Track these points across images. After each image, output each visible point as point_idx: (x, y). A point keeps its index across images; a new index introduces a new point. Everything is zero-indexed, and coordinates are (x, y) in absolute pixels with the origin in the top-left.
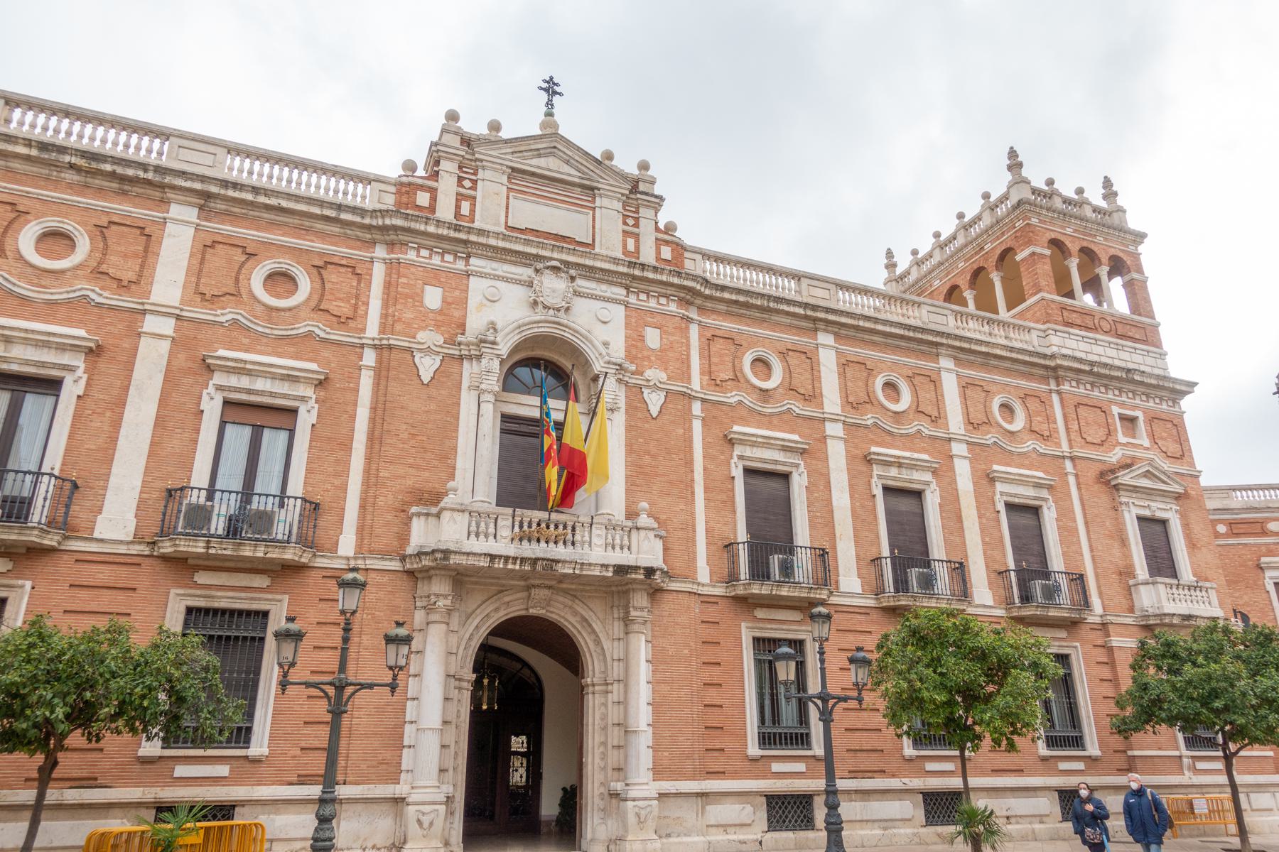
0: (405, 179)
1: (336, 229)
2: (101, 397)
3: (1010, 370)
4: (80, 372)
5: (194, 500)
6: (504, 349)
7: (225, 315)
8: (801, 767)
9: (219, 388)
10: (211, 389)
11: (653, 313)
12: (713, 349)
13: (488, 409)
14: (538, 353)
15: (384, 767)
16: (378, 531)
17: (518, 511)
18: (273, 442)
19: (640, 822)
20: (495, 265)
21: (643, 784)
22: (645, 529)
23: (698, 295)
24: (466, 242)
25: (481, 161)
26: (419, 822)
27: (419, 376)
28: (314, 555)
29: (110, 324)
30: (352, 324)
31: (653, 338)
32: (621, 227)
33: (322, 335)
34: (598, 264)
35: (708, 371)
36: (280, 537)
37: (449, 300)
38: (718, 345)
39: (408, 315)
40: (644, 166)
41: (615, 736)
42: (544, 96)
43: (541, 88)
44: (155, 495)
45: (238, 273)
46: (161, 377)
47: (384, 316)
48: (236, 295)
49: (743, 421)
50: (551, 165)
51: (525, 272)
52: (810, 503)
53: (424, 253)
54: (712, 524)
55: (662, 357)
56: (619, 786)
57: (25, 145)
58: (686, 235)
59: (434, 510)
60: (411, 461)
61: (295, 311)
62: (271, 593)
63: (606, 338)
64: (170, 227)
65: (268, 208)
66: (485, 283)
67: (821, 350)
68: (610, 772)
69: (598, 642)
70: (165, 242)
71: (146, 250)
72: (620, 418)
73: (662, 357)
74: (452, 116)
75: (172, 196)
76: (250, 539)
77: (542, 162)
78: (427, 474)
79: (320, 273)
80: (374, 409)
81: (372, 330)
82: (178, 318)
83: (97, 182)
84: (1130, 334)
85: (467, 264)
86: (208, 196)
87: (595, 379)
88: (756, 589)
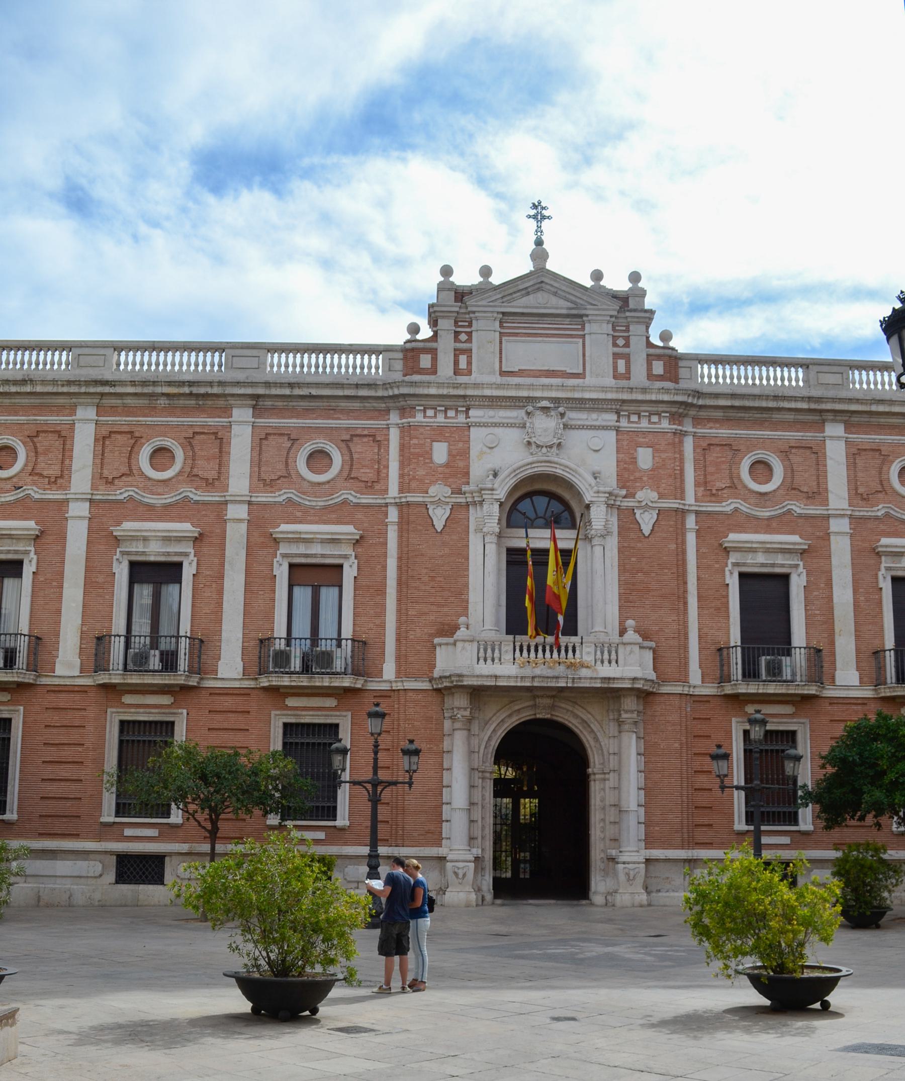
0: (409, 345)
1: (357, 405)
2: (208, 573)
4: (192, 557)
5: (277, 647)
6: (501, 493)
7: (280, 497)
8: (786, 840)
9: (284, 556)
10: (279, 558)
11: (644, 433)
12: (709, 458)
13: (491, 548)
14: (538, 486)
15: (430, 835)
16: (411, 659)
17: (518, 637)
18: (328, 595)
19: (629, 880)
20: (491, 413)
21: (633, 853)
22: (631, 644)
23: (693, 407)
24: (464, 397)
25: (474, 312)
26: (456, 874)
27: (433, 525)
28: (366, 681)
29: (206, 515)
30: (377, 487)
31: (645, 458)
32: (611, 350)
33: (355, 500)
34: (587, 395)
35: (703, 483)
36: (338, 670)
37: (454, 452)
38: (714, 455)
39: (421, 472)
40: (635, 277)
41: (612, 815)
42: (533, 223)
43: (529, 217)
44: (253, 643)
45: (287, 458)
46: (243, 553)
47: (402, 476)
48: (288, 476)
49: (741, 529)
51: (517, 415)
52: (808, 602)
53: (430, 413)
54: (705, 630)
55: (654, 477)
56: (614, 852)
57: (132, 386)
58: (681, 344)
59: (451, 640)
60: (432, 600)
61: (332, 483)
62: (339, 710)
63: (597, 468)
64: (235, 429)
65: (302, 397)
66: (484, 431)
67: (828, 442)
68: (608, 842)
69: (596, 739)
70: (234, 441)
71: (221, 452)
72: (613, 542)
73: (654, 477)
74: (447, 271)
75: (233, 402)
76: (318, 673)
77: (530, 300)
78: (446, 609)
79: (348, 447)
80: (400, 559)
81: (393, 490)
82: (250, 503)
83: (181, 402)
85: (467, 417)
86: (257, 397)
87: (588, 507)
88: (743, 689)
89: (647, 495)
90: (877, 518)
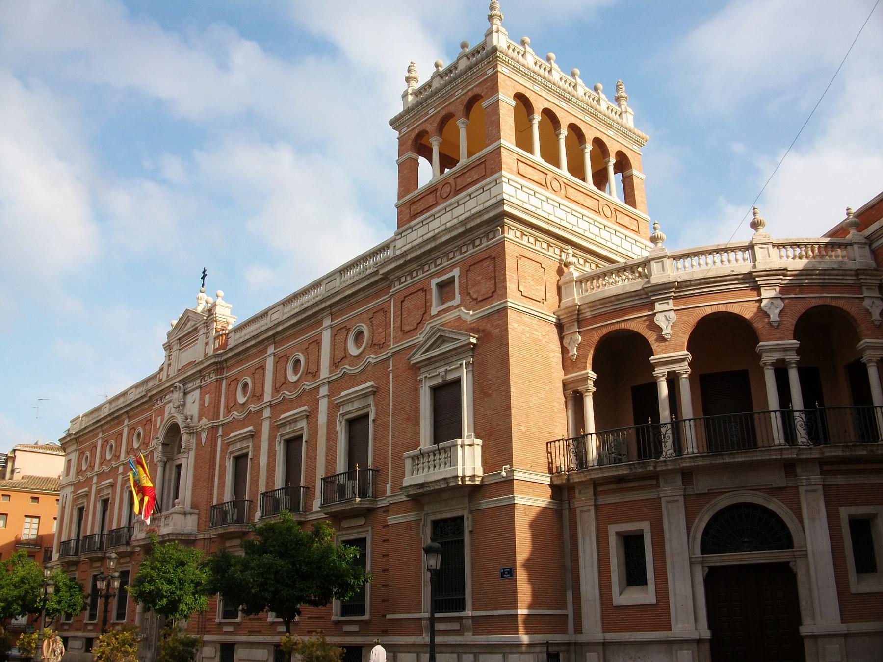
3: (366, 297)
35: (226, 407)
50: (189, 327)
84: (469, 180)
89: (204, 421)
90: (280, 402)
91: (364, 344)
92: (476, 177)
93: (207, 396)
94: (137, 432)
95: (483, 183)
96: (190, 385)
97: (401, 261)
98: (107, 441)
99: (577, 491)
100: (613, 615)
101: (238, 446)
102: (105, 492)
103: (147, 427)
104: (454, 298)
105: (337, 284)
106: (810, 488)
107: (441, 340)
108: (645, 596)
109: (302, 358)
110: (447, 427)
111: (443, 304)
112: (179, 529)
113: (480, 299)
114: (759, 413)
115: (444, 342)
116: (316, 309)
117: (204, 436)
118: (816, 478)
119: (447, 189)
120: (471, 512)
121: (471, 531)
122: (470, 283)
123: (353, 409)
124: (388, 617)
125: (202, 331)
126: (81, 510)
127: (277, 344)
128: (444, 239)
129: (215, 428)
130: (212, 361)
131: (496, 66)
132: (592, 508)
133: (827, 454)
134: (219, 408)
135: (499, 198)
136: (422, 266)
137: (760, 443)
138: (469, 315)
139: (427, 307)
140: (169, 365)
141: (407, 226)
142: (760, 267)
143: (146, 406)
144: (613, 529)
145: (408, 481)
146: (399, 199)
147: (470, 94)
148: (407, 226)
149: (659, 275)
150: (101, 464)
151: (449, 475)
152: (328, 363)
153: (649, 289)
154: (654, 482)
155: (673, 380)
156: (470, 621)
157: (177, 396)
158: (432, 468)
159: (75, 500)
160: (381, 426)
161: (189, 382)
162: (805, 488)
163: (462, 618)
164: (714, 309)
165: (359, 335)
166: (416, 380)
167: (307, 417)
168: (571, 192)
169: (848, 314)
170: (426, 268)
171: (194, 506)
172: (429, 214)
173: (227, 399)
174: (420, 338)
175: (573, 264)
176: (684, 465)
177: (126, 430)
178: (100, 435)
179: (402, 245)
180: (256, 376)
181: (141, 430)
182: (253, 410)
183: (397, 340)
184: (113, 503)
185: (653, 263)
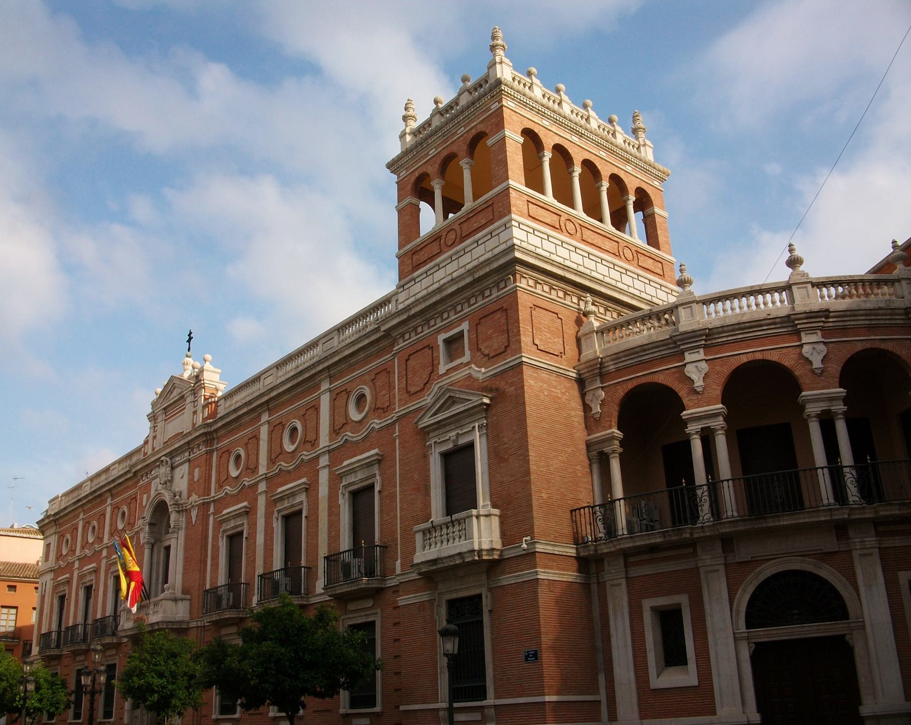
3: (368, 357)
35: (218, 481)
84: (476, 225)
89: (194, 497)
90: (277, 475)
91: (367, 409)
92: (483, 222)
93: (197, 470)
94: (121, 511)
95: (491, 227)
96: (178, 459)
97: (405, 317)
98: (89, 523)
99: (606, 563)
100: (653, 702)
101: (232, 524)
102: (88, 578)
103: (132, 506)
104: (464, 355)
105: (335, 343)
106: (866, 551)
107: (450, 402)
108: (684, 677)
109: (299, 426)
110: (459, 497)
111: (452, 361)
112: (170, 617)
113: (492, 355)
114: (804, 470)
115: (454, 403)
116: (314, 371)
117: (194, 514)
118: (871, 541)
119: (452, 236)
120: (490, 589)
121: (490, 611)
122: (480, 337)
123: (357, 479)
124: (402, 708)
125: (190, 399)
126: (62, 598)
127: (271, 411)
128: (450, 291)
129: (206, 505)
130: (202, 431)
131: (500, 101)
132: (623, 582)
133: (882, 513)
134: (210, 482)
135: (509, 244)
136: (427, 321)
137: (807, 504)
138: (481, 373)
139: (434, 365)
140: (155, 437)
141: (410, 277)
142: (799, 308)
143: (130, 483)
144: (648, 604)
145: (420, 557)
146: (400, 248)
147: (474, 132)
148: (410, 277)
149: (687, 322)
150: (83, 548)
151: (464, 550)
152: (328, 431)
153: (678, 338)
154: (691, 550)
155: (707, 437)
156: (493, 710)
157: (164, 470)
158: (445, 543)
159: (55, 587)
160: (388, 497)
161: (177, 455)
162: (859, 552)
163: (483, 707)
164: (750, 357)
165: (361, 398)
166: (425, 445)
167: (307, 489)
168: (588, 234)
169: (899, 357)
170: (432, 322)
171: (185, 591)
172: (432, 264)
173: (219, 473)
174: (428, 400)
175: (594, 313)
176: (724, 530)
177: (109, 509)
178: (81, 516)
179: (404, 300)
180: (250, 446)
181: (125, 509)
182: (247, 484)
183: (403, 402)
184: (97, 590)
185: (680, 309)
